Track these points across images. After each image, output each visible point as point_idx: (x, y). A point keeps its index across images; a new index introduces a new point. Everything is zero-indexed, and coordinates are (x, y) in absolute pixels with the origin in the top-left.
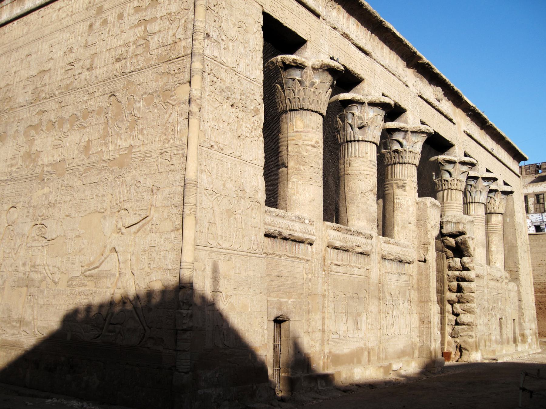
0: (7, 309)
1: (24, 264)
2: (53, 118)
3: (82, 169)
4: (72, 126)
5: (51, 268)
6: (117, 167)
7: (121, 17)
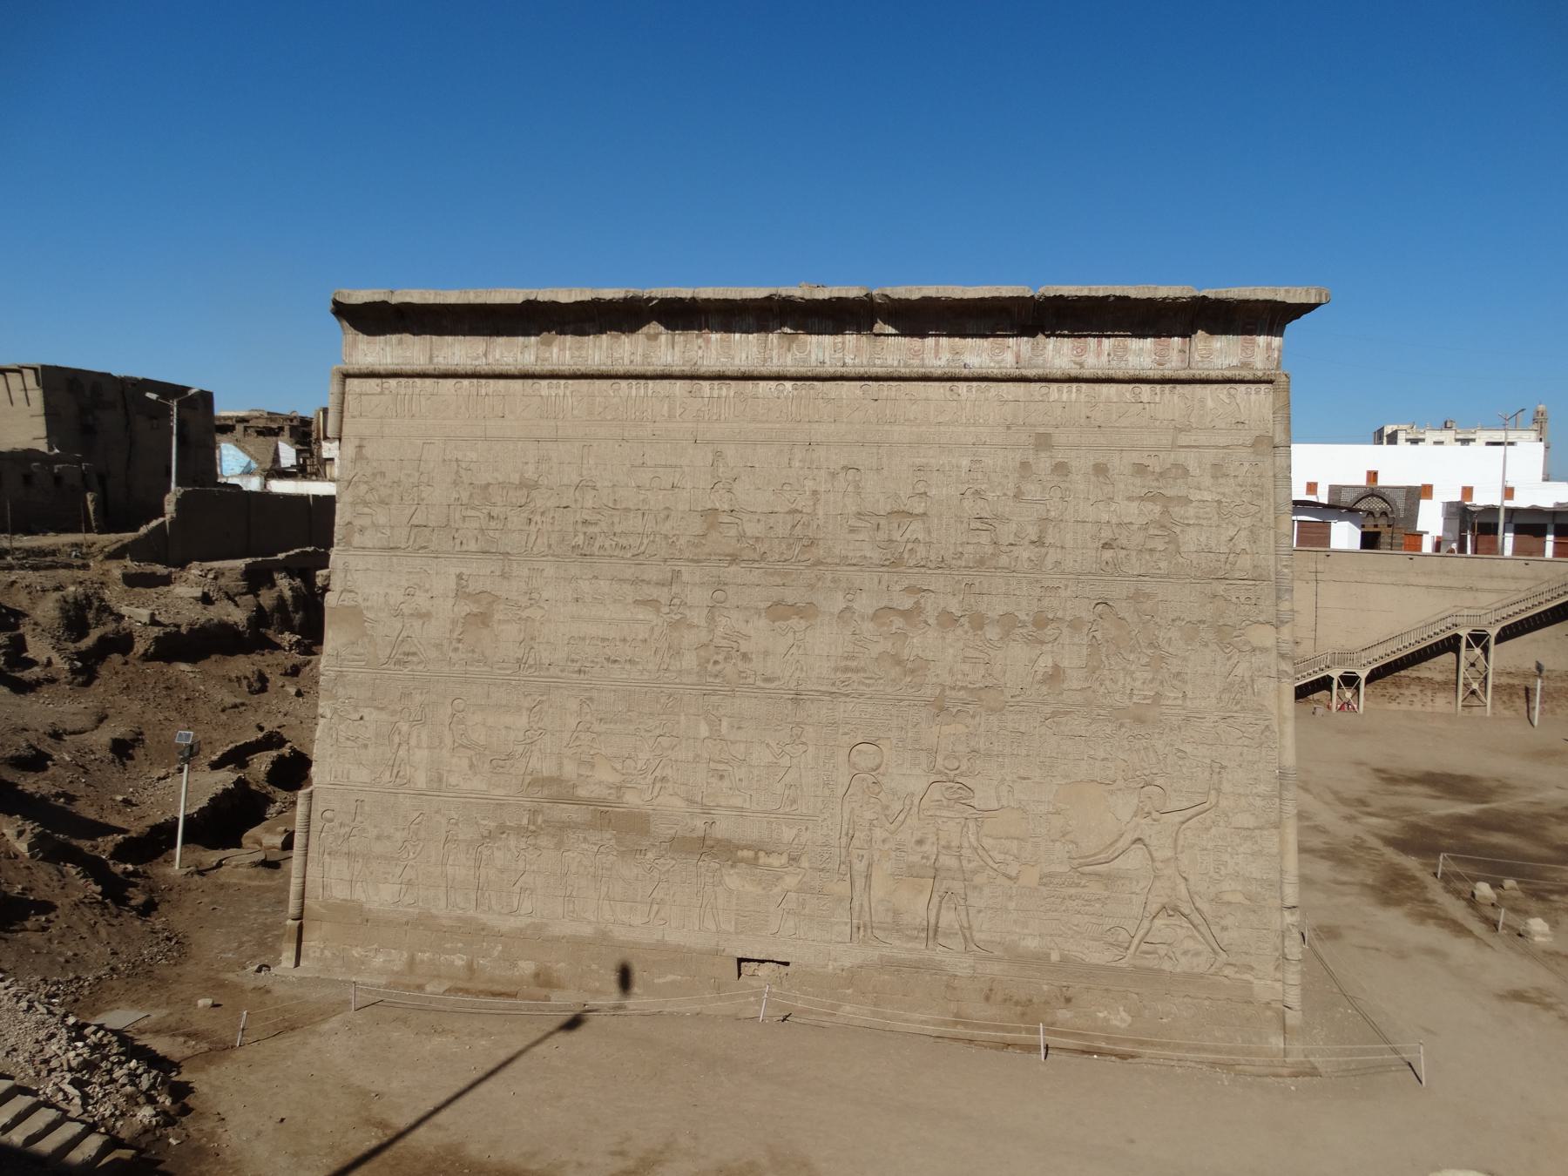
1: (920, 842)
2: (954, 607)
4: (1006, 635)
5: (994, 853)
7: (1100, 470)
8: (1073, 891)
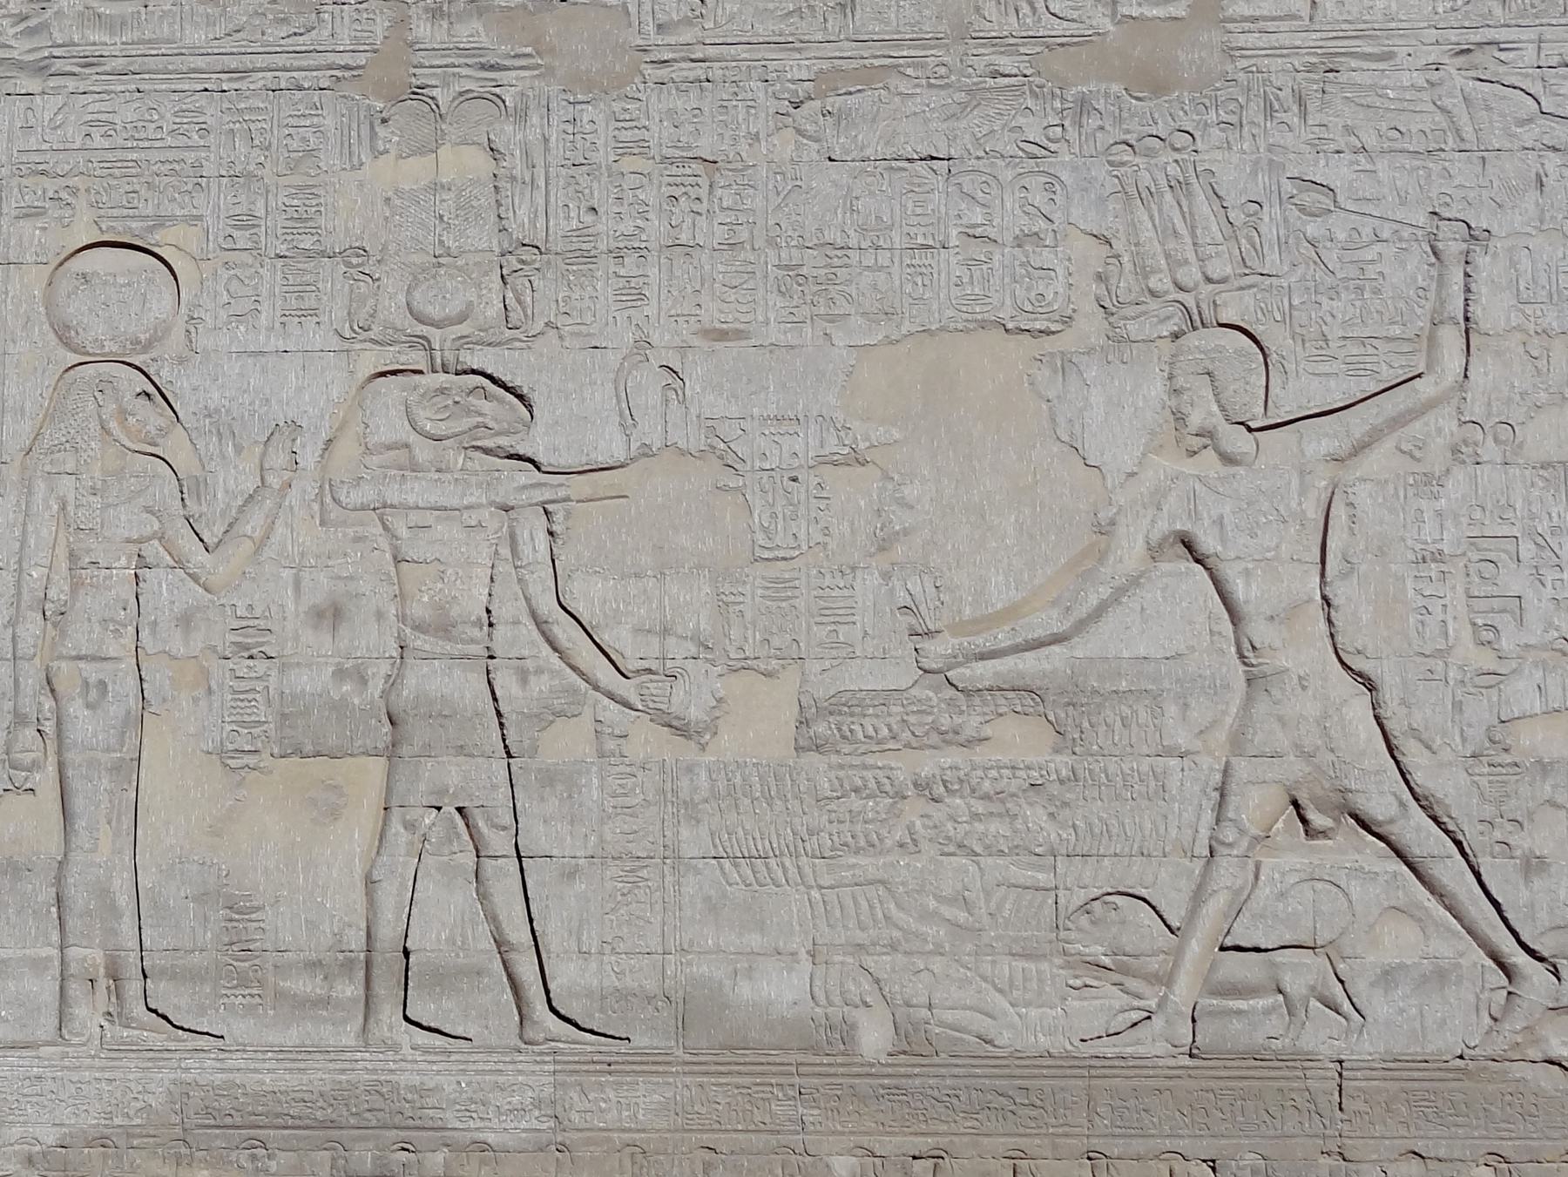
0: (201, 898)
3: (798, 67)
6: (1116, 88)
8: (928, 765)
